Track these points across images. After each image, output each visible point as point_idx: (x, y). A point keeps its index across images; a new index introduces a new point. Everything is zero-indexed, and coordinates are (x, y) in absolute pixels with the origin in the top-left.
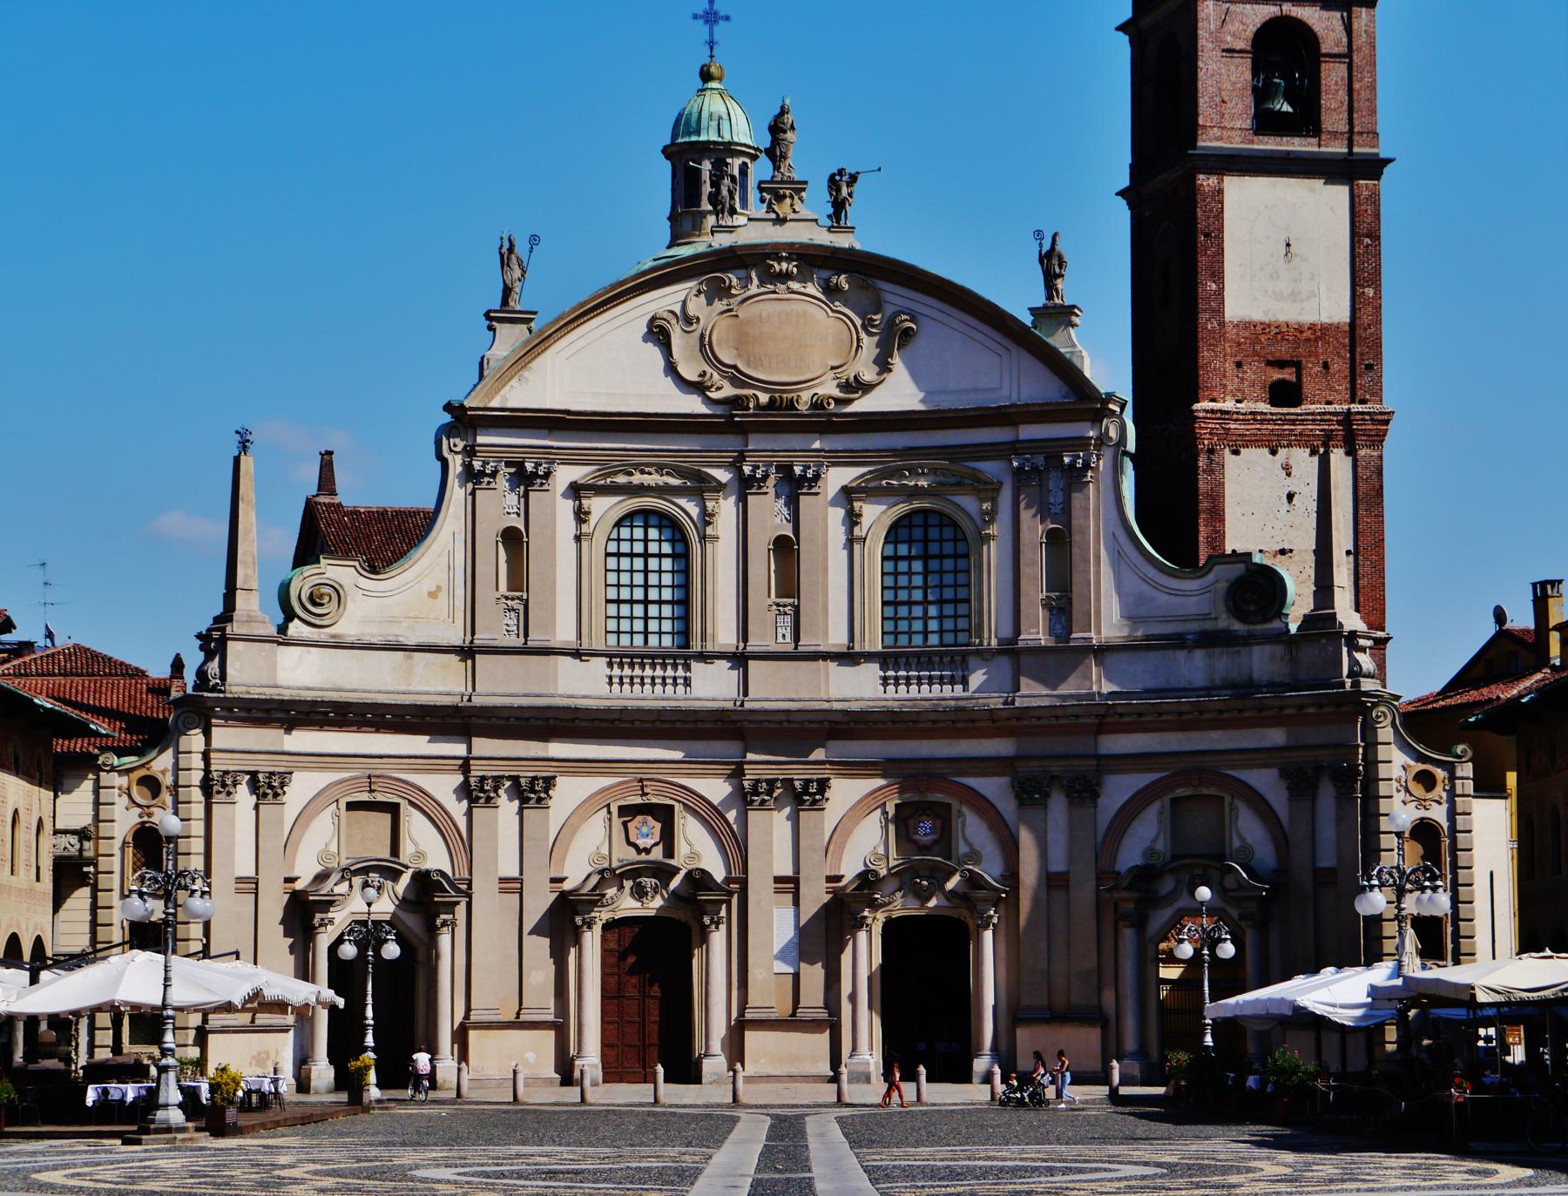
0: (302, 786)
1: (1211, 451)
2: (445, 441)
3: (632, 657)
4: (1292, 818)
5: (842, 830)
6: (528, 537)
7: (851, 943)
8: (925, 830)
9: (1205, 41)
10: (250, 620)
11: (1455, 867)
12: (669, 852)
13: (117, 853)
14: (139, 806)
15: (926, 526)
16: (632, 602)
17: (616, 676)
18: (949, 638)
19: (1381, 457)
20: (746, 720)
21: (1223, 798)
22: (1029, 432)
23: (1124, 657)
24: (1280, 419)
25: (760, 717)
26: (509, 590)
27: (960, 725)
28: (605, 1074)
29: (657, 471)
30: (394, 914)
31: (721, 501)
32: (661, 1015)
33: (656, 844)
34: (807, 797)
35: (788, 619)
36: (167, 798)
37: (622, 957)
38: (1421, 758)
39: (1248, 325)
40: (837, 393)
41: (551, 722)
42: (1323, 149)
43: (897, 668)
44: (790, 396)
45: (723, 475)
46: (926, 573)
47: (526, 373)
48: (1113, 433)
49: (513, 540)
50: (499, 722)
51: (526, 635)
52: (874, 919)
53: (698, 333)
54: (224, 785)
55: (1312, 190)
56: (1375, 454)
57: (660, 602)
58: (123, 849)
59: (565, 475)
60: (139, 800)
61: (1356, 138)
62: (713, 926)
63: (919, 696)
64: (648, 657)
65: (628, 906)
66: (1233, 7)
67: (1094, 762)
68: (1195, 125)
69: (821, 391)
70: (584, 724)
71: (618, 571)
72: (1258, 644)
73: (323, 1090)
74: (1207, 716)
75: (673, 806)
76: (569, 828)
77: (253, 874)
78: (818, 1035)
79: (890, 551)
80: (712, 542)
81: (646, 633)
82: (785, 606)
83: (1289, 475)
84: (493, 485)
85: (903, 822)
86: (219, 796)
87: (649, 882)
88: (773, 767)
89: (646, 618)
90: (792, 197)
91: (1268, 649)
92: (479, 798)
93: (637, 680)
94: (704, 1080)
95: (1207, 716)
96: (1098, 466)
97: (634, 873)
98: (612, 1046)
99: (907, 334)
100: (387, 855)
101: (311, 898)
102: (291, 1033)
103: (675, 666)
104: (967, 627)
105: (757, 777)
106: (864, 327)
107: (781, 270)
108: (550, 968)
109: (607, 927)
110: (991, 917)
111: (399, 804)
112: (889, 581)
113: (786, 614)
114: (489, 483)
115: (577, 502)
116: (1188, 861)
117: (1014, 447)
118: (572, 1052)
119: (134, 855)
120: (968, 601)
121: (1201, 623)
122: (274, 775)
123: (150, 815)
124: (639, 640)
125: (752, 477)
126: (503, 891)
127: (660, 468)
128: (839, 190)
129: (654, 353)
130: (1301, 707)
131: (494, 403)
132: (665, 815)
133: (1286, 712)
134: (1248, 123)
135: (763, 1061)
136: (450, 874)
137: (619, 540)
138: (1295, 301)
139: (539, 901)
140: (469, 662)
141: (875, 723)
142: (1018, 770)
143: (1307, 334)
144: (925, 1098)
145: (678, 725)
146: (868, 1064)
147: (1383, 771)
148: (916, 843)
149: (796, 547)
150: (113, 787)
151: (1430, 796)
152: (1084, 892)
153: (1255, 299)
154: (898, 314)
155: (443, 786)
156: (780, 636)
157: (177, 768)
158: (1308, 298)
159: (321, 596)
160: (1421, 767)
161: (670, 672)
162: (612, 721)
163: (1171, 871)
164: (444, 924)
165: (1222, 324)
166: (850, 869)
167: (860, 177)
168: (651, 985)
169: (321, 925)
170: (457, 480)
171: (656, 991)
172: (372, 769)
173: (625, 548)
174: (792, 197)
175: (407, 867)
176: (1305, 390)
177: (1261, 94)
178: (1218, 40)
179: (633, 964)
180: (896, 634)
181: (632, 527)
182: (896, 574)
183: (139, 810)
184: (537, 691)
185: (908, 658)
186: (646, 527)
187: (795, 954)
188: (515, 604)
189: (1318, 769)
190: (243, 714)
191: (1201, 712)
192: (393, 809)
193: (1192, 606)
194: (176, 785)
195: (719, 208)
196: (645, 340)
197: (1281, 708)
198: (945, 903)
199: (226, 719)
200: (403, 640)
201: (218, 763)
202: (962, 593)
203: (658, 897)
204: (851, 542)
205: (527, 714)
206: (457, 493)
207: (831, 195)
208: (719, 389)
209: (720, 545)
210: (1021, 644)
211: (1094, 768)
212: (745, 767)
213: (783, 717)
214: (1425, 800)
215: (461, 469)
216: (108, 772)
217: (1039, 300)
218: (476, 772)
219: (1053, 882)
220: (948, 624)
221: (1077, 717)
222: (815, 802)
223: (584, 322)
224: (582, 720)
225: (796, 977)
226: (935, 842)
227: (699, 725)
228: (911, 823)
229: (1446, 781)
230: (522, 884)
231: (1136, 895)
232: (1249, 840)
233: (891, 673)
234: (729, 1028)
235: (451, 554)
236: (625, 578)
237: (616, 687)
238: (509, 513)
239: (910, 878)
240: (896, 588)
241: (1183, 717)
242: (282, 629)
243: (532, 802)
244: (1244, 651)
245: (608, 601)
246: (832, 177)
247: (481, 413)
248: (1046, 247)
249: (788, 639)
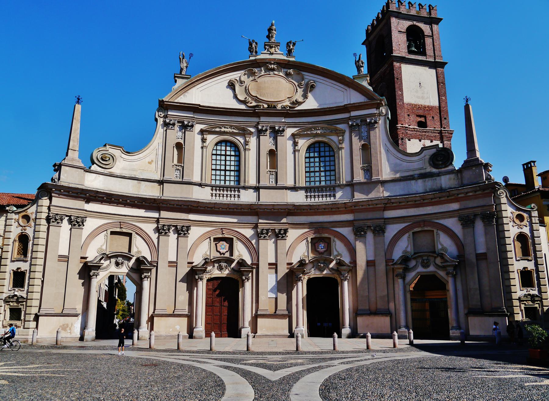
0: (91, 224)
1: (402, 139)
2: (157, 113)
3: (220, 187)
4: (464, 235)
5: (292, 247)
6: (184, 146)
7: (296, 286)
8: (321, 247)
9: (393, 28)
10: (73, 160)
11: (535, 251)
12: (232, 254)
13: (11, 243)
14: (22, 226)
15: (319, 147)
16: (220, 170)
17: (214, 194)
18: (328, 183)
19: (451, 144)
20: (259, 208)
21: (433, 231)
22: (353, 114)
23: (391, 184)
24: (422, 131)
25: (264, 207)
26: (178, 163)
27: (334, 210)
28: (206, 334)
29: (230, 128)
30: (127, 273)
31: (251, 138)
32: (228, 313)
33: (227, 252)
34: (280, 235)
35: (273, 176)
36: (33, 224)
37: (215, 290)
38: (518, 209)
39: (410, 104)
40: (290, 105)
41: (190, 207)
42: (427, 60)
43: (311, 192)
44: (274, 104)
45: (252, 130)
46: (320, 162)
47: (186, 94)
48: (384, 111)
49: (179, 147)
50: (170, 206)
51: (183, 178)
52: (304, 278)
53: (244, 86)
54: (56, 220)
55: (426, 70)
56: (449, 143)
57: (230, 171)
58: (13, 243)
59: (198, 127)
60: (22, 224)
61: (436, 57)
62: (246, 280)
63: (319, 201)
64: (225, 187)
65: (215, 272)
66: (400, 21)
67: (383, 220)
68: (392, 50)
69: (284, 104)
70: (201, 208)
71: (216, 160)
72: (443, 175)
73: (90, 340)
74: (426, 201)
75: (233, 238)
76: (196, 245)
77: (67, 255)
78: (284, 320)
79: (307, 155)
80: (248, 151)
81: (225, 180)
82: (272, 172)
84: (173, 128)
85: (314, 243)
86: (53, 223)
87: (223, 264)
88: (268, 225)
89: (225, 176)
90: (275, 47)
91: (448, 176)
92: (162, 232)
93: (221, 195)
94: (242, 337)
95: (426, 201)
96: (379, 122)
97: (218, 261)
98: (209, 324)
99: (313, 87)
100: (127, 252)
101: (89, 264)
102: (80, 317)
103: (235, 191)
104: (334, 179)
105: (263, 228)
106: (298, 85)
107: (271, 67)
108: (187, 294)
109: (208, 280)
110: (347, 276)
111: (132, 233)
112: (308, 165)
113: (273, 175)
114: (172, 127)
115: (202, 136)
116: (422, 254)
117: (350, 118)
118: (194, 326)
119: (19, 245)
120: (335, 170)
121: (420, 171)
122: (79, 218)
123: (25, 230)
125: (262, 130)
126: (169, 266)
127: (231, 127)
128: (290, 47)
129: (230, 92)
130: (467, 193)
131: (176, 101)
132: (230, 241)
133: (460, 196)
134: (407, 51)
135: (264, 329)
136: (149, 260)
137: (216, 150)
138: (423, 99)
139: (184, 270)
140: (162, 186)
141: (304, 210)
142: (355, 224)
143: (427, 108)
144: (338, 348)
145: (235, 210)
146: (303, 331)
147: (504, 214)
148: (318, 252)
149: (276, 153)
150: (12, 219)
151: (522, 223)
152: (381, 267)
154: (310, 81)
155: (149, 228)
156: (271, 182)
157: (37, 212)
158: (427, 99)
159: (106, 157)
160: (518, 213)
161: (233, 193)
162: (212, 208)
163: (414, 258)
164: (145, 277)
165: (403, 103)
166: (295, 260)
168: (224, 301)
169: (93, 275)
170: (161, 126)
171: (226, 304)
172: (121, 220)
173: (219, 152)
174: (275, 47)
175: (133, 256)
176: (427, 124)
177: (409, 47)
178: (397, 28)
179: (218, 294)
180: (310, 182)
181: (221, 146)
182: (310, 162)
183: (21, 228)
184: (185, 197)
185: (314, 189)
186: (226, 146)
187: (276, 291)
188: (179, 168)
189: (475, 216)
190: (67, 193)
191: (424, 200)
192: (129, 235)
193: (416, 165)
194: (36, 218)
195: (252, 50)
196: (227, 87)
198: (329, 272)
199: (59, 194)
200: (137, 177)
201: (54, 210)
202: (332, 168)
203: (227, 270)
204: (294, 151)
205: (180, 203)
206: (160, 130)
207: (287, 48)
208: (251, 103)
209: (251, 152)
210: (354, 182)
211: (383, 222)
212: (259, 224)
213: (271, 207)
214: (521, 225)
215: (162, 123)
216: (11, 213)
217: (356, 73)
218: (162, 222)
219: (370, 264)
220: (328, 178)
221: (376, 204)
222: (283, 237)
223: (207, 80)
224: (201, 207)
225: (276, 299)
226: (325, 251)
227: (243, 210)
228: (316, 245)
229: (528, 218)
230: (177, 264)
231: (404, 266)
232: (445, 245)
233: (309, 194)
234: (252, 317)
235: (157, 150)
236: (218, 162)
237: (214, 197)
238: (178, 138)
239: (315, 263)
240: (310, 167)
241: (417, 202)
242: (90, 168)
243: (182, 235)
244: (438, 178)
245: (212, 170)
246: (288, 43)
247: (169, 103)
248: (357, 59)
249: (273, 183)
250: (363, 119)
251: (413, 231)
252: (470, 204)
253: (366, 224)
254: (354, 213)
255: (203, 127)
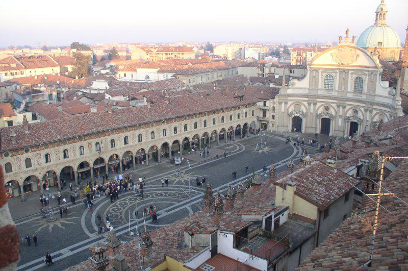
255: (322, 70)
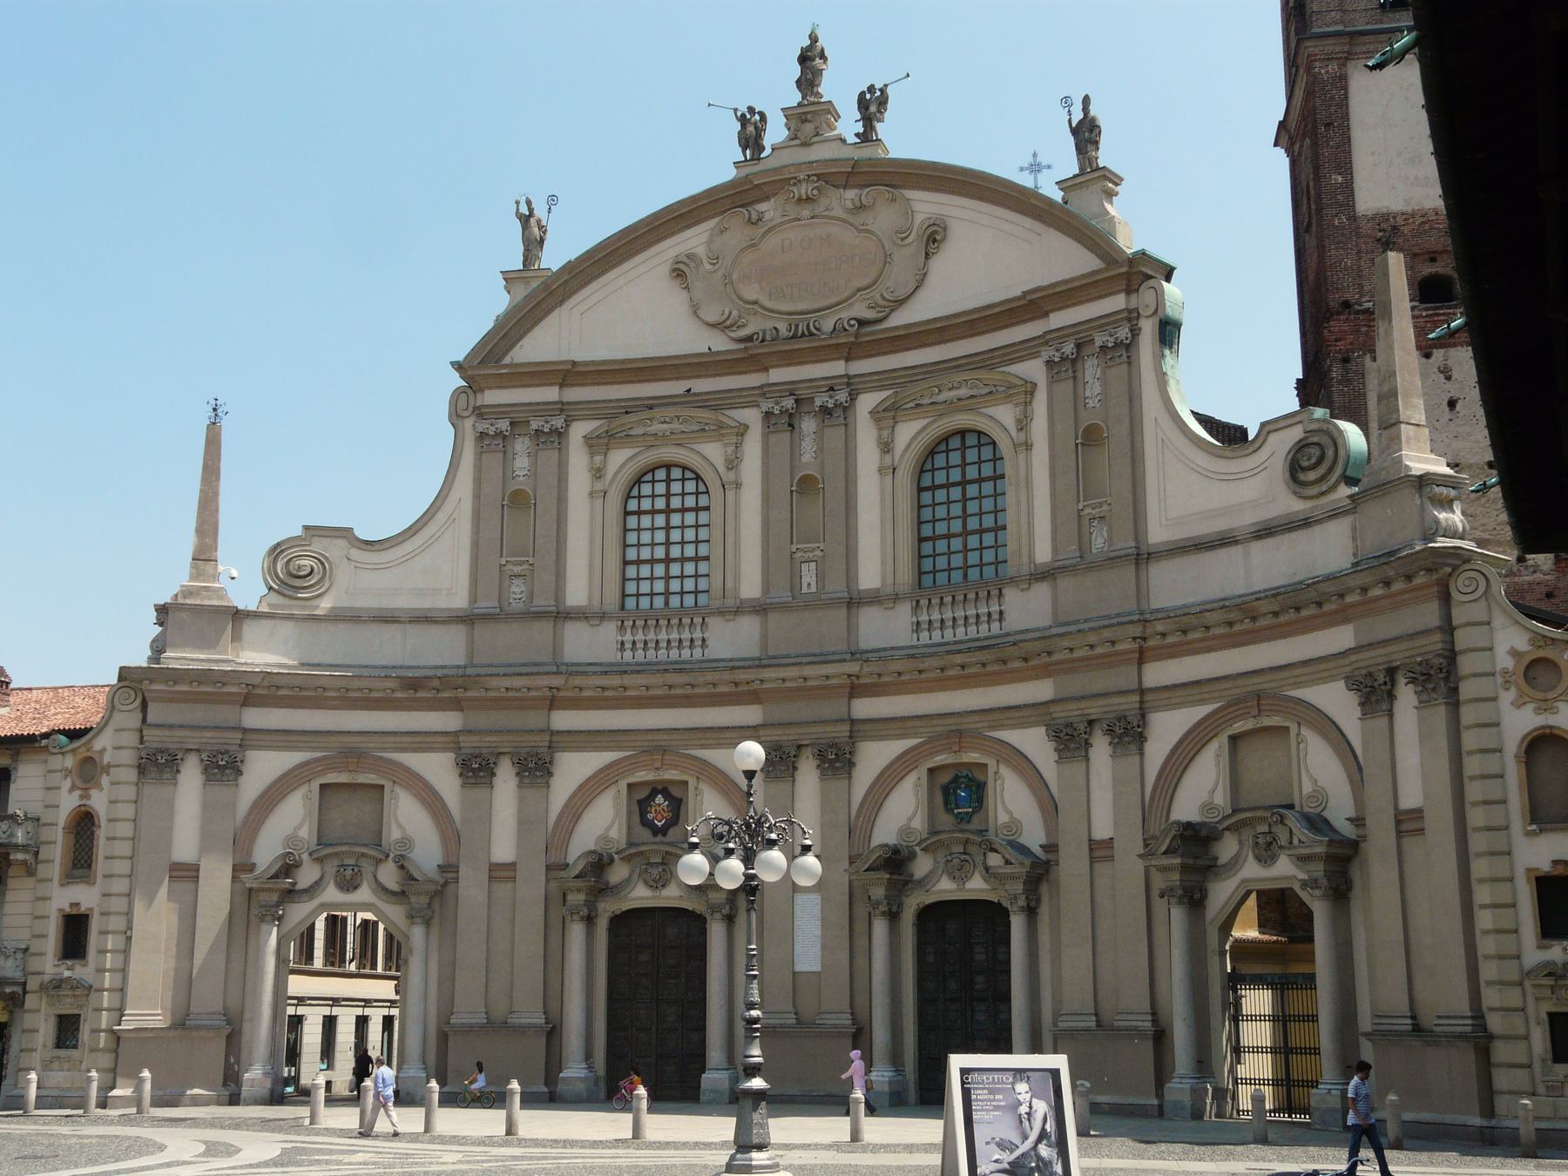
1: (1346, 360)
69: (845, 315)
83: (1449, 378)
116: (1248, 815)
123: (88, 797)
124: (659, 602)
133: (1349, 599)
153: (1394, 188)
163: (1236, 828)
165: (1353, 218)
167: (889, 90)
172: (352, 751)
189: (1391, 672)
197: (1342, 596)
231: (1177, 861)
246: (862, 94)
248: (1078, 116)
250: (1081, 337)
251: (1231, 733)
252: (1385, 626)
253: (1086, 711)
254: (1049, 676)
